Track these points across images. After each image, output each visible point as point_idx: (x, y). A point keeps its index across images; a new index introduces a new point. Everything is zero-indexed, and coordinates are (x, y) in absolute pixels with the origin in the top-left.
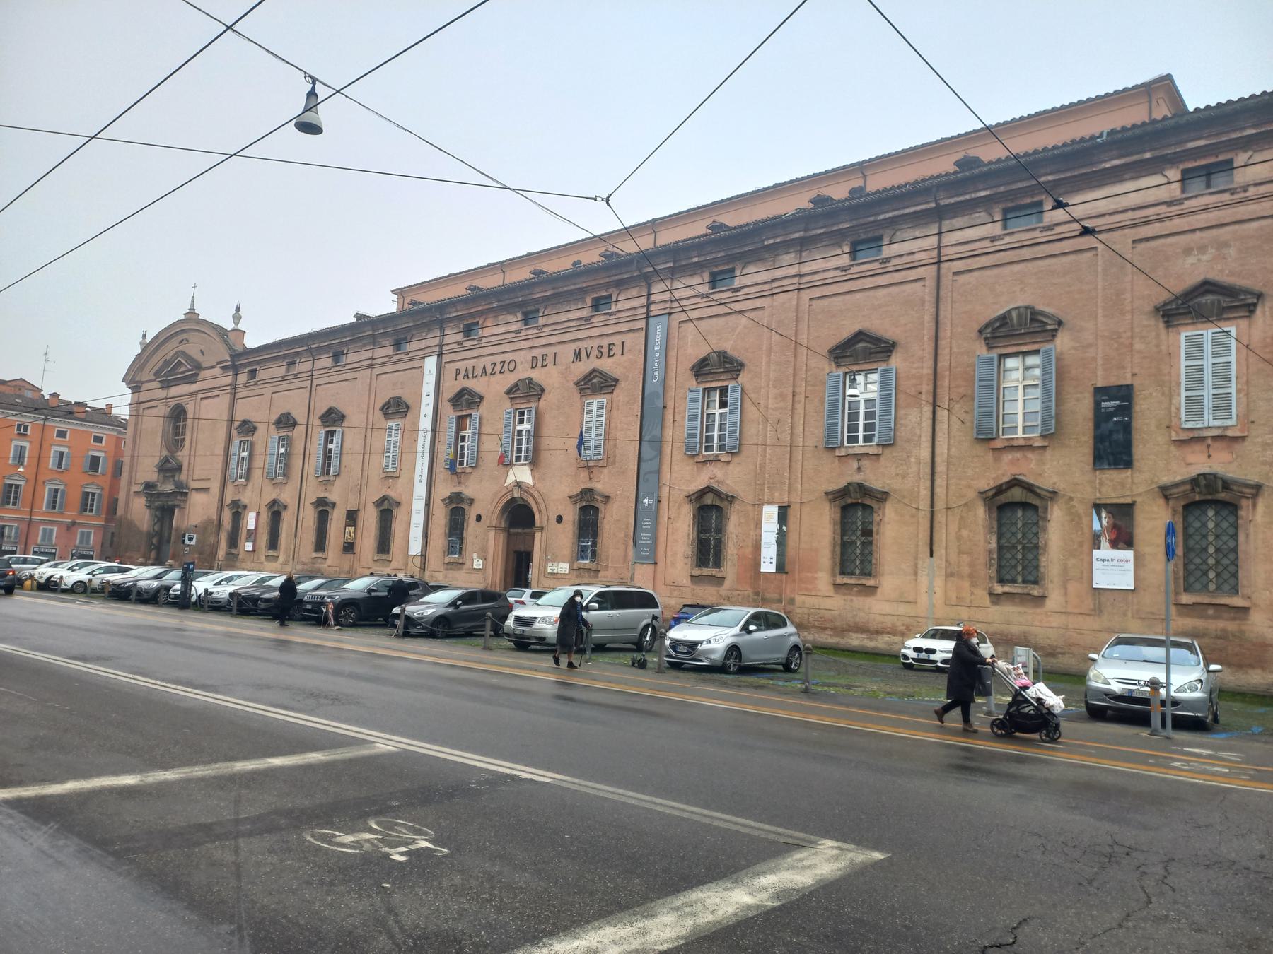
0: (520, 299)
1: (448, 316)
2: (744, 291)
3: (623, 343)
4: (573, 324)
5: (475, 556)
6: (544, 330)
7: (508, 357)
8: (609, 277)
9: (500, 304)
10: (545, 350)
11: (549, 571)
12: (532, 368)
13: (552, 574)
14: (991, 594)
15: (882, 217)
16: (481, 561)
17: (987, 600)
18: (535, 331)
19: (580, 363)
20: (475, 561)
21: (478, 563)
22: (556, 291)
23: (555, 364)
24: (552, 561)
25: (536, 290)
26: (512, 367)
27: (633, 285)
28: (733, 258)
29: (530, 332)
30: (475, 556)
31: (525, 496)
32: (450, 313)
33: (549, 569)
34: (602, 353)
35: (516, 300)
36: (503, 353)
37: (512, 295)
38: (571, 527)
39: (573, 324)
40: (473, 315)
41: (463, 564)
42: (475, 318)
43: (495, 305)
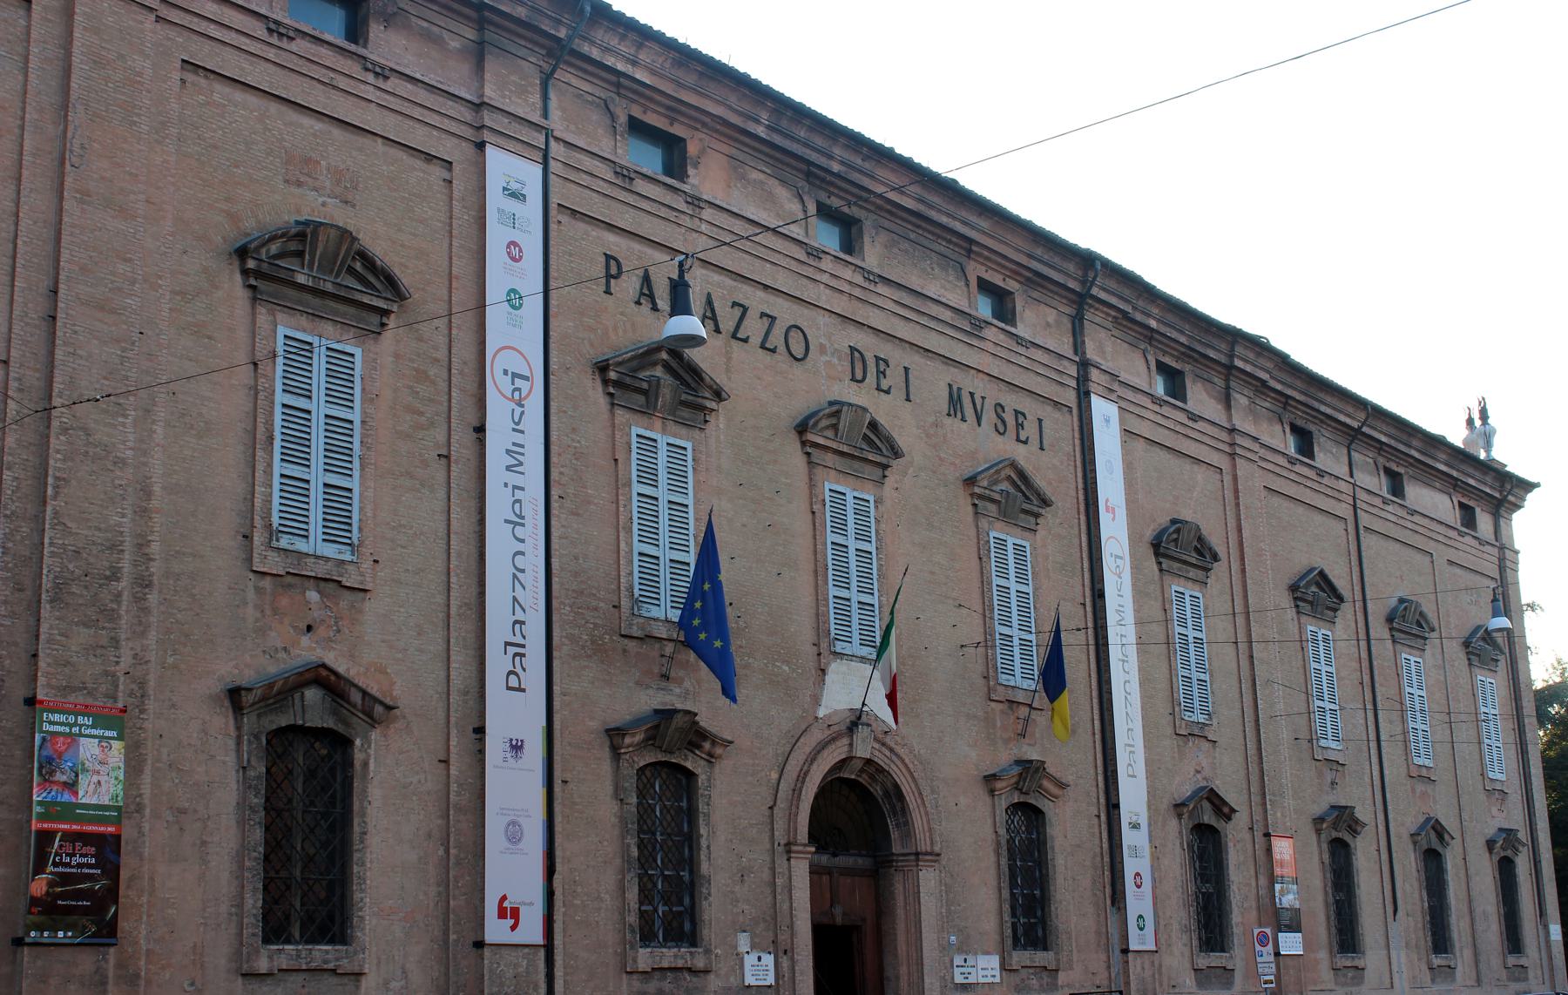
0: (836, 167)
1: (595, 54)
2: (1200, 425)
3: (1040, 421)
4: (947, 315)
5: (743, 942)
6: (881, 289)
7: (786, 313)
8: (1030, 256)
9: (778, 139)
10: (886, 350)
11: (959, 979)
12: (853, 379)
13: (965, 987)
14: (1431, 969)
15: (1323, 408)
16: (769, 960)
17: (1427, 976)
18: (859, 279)
19: (964, 426)
20: (750, 960)
21: (759, 969)
22: (921, 208)
23: (908, 399)
24: (960, 950)
25: (882, 173)
26: (798, 350)
27: (1049, 301)
28: (1189, 354)
29: (847, 273)
30: (743, 942)
31: (880, 760)
32: (607, 50)
33: (957, 971)
34: (1004, 422)
35: (823, 161)
36: (766, 287)
37: (819, 141)
38: (993, 858)
39: (947, 315)
40: (675, 109)
41: (707, 972)
42: (672, 121)
43: (761, 131)
